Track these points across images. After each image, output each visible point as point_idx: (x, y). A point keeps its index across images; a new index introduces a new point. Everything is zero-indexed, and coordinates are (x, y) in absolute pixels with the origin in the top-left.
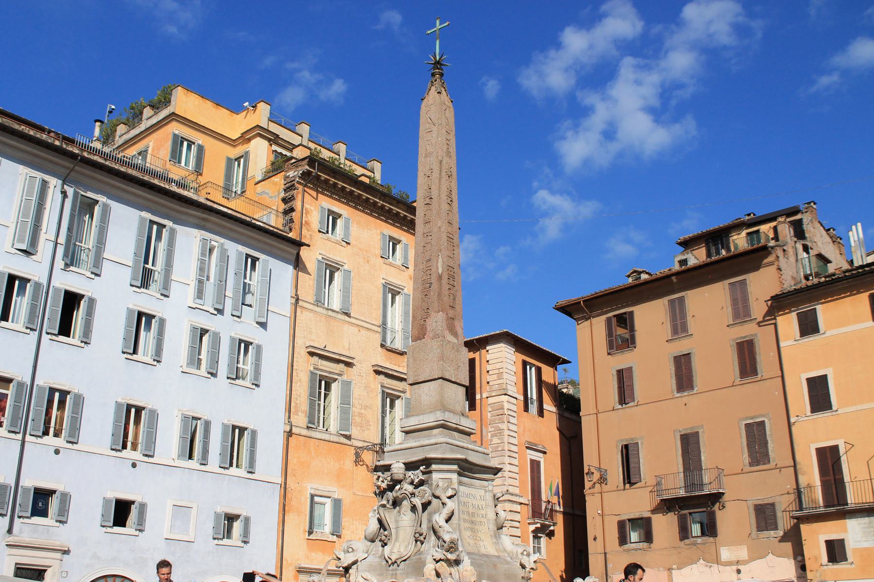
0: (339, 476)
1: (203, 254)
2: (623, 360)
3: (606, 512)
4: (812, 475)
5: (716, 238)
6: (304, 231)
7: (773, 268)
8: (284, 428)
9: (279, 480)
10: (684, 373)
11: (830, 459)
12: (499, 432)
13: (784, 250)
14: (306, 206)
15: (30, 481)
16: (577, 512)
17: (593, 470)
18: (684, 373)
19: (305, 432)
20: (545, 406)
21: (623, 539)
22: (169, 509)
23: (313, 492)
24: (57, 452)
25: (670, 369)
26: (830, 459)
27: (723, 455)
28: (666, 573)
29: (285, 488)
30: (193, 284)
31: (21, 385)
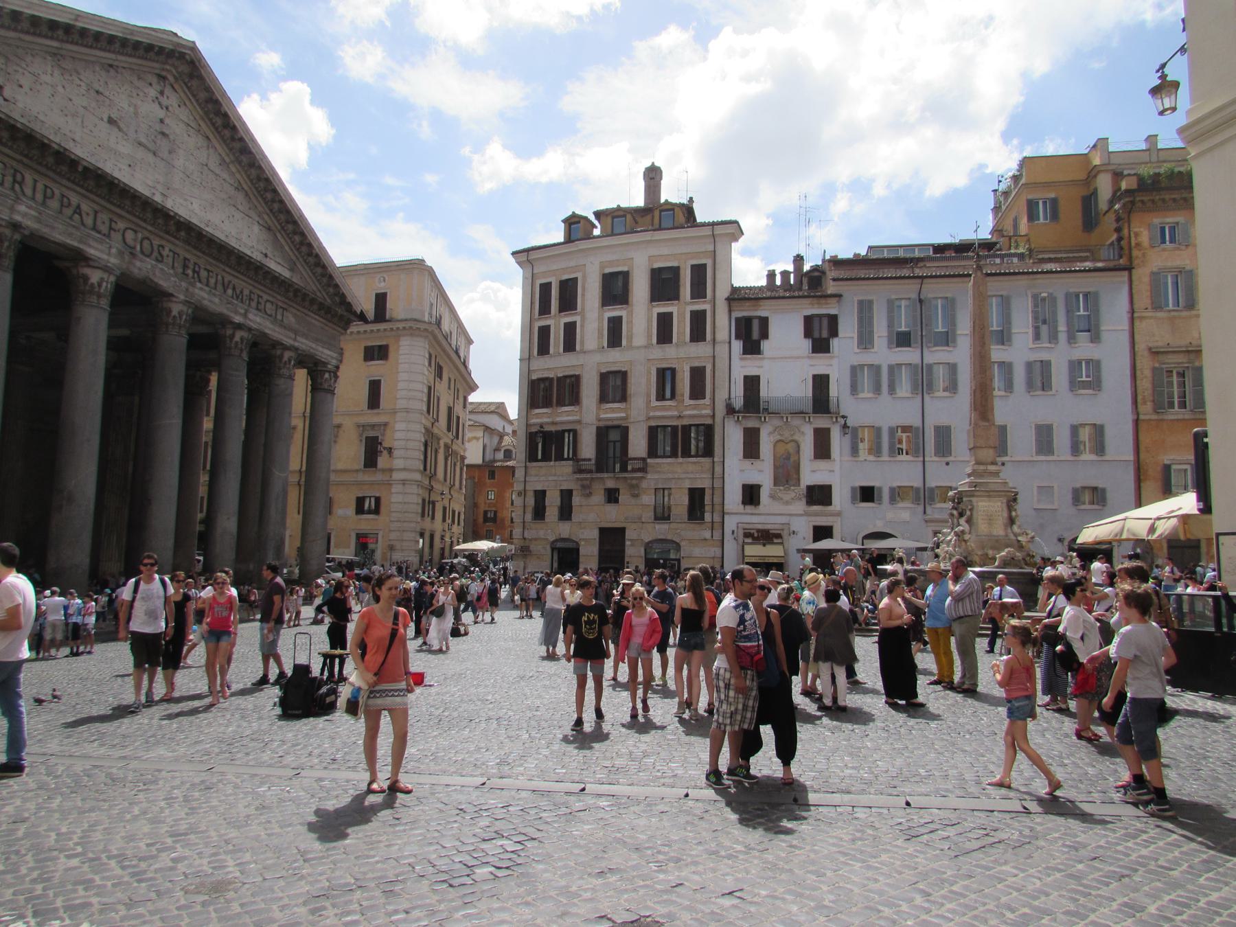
1: (1036, 306)
6: (1135, 253)
8: (1129, 418)
9: (1131, 458)
15: (931, 483)
19: (1154, 417)
24: (947, 464)
30: (1031, 331)
31: (917, 428)
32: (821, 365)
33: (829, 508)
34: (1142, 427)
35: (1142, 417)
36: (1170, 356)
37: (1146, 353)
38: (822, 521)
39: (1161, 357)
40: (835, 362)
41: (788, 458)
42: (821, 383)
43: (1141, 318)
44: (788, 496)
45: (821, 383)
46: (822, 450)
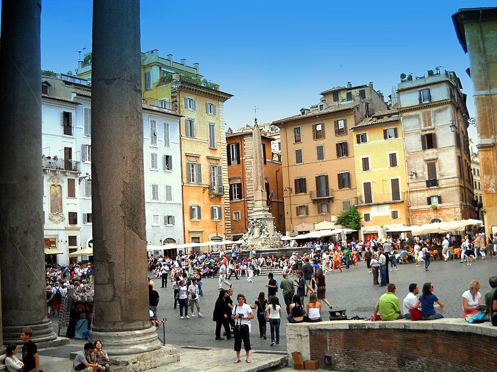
0: (198, 199)
2: (298, 147)
3: (292, 204)
4: (361, 192)
5: (335, 93)
7: (353, 117)
8: (181, 184)
10: (320, 155)
11: (367, 186)
12: (250, 174)
13: (358, 108)
14: (181, 99)
16: (280, 201)
17: (287, 189)
18: (320, 155)
20: (267, 160)
21: (298, 214)
22: (152, 216)
23: (191, 205)
25: (315, 151)
26: (367, 186)
27: (333, 183)
28: (313, 225)
29: (183, 205)
32: (68, 142)
33: (77, 226)
34: (184, 187)
35: (185, 184)
36: (191, 158)
37: (184, 155)
38: (73, 234)
39: (189, 158)
40: (74, 141)
41: (56, 196)
42: (68, 151)
43: (183, 139)
44: (57, 218)
45: (68, 151)
46: (72, 194)
